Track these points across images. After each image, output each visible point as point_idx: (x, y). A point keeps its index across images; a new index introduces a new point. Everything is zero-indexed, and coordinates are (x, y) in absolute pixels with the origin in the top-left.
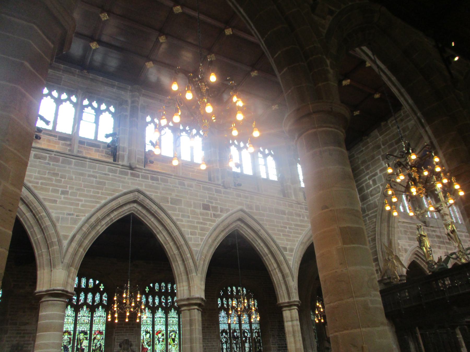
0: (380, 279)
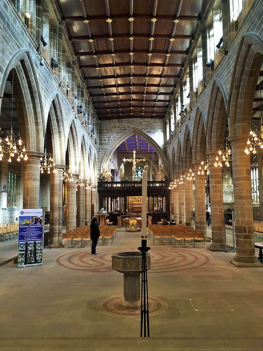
0: (99, 177)
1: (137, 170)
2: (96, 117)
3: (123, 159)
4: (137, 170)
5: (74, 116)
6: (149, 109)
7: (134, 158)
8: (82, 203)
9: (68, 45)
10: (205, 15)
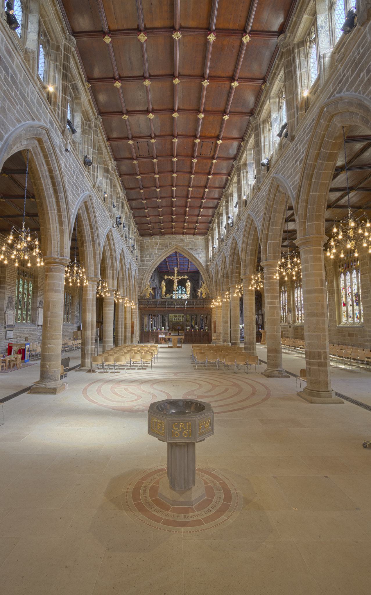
2: (137, 234)
3: (165, 275)
5: (111, 225)
6: (192, 226)
7: (176, 275)
8: (121, 321)
9: (106, 147)
10: (258, 109)
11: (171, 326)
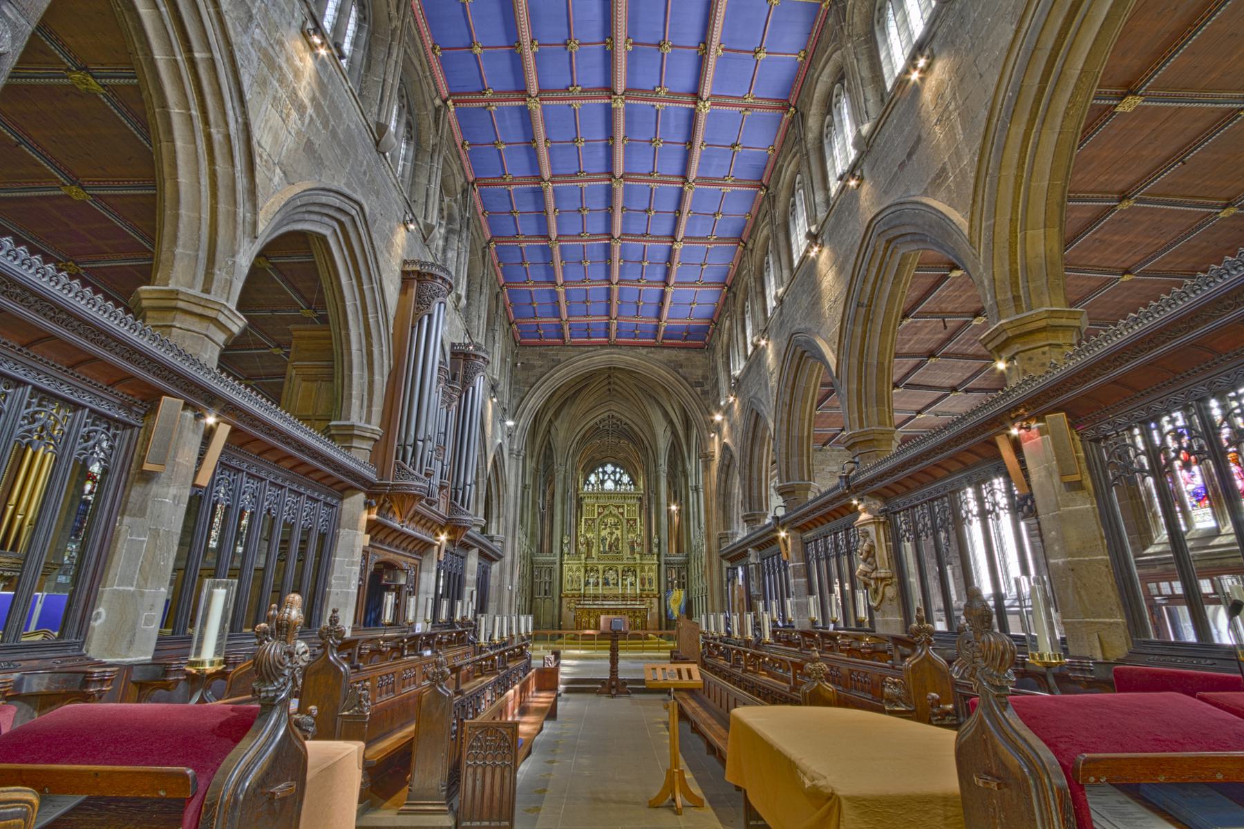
1: (601, 475)
4: (601, 475)
11: (572, 615)
